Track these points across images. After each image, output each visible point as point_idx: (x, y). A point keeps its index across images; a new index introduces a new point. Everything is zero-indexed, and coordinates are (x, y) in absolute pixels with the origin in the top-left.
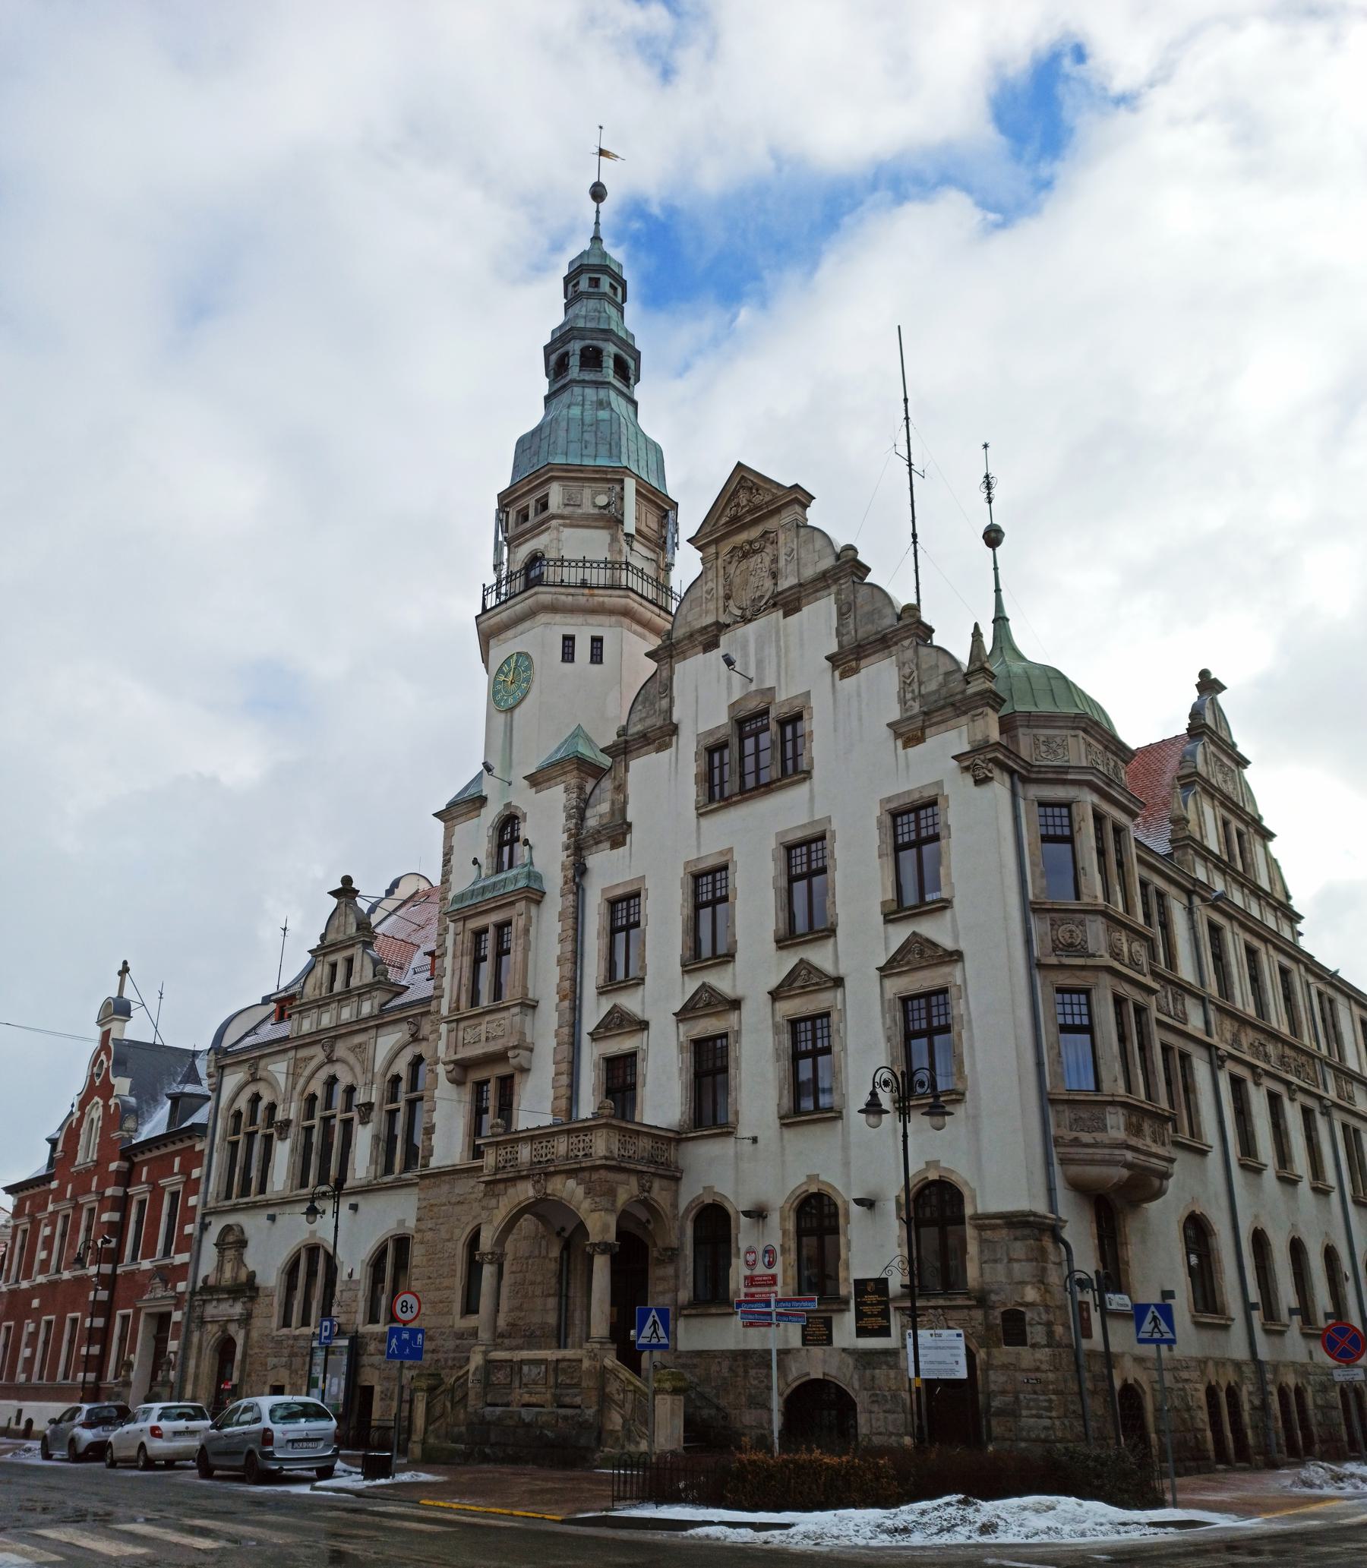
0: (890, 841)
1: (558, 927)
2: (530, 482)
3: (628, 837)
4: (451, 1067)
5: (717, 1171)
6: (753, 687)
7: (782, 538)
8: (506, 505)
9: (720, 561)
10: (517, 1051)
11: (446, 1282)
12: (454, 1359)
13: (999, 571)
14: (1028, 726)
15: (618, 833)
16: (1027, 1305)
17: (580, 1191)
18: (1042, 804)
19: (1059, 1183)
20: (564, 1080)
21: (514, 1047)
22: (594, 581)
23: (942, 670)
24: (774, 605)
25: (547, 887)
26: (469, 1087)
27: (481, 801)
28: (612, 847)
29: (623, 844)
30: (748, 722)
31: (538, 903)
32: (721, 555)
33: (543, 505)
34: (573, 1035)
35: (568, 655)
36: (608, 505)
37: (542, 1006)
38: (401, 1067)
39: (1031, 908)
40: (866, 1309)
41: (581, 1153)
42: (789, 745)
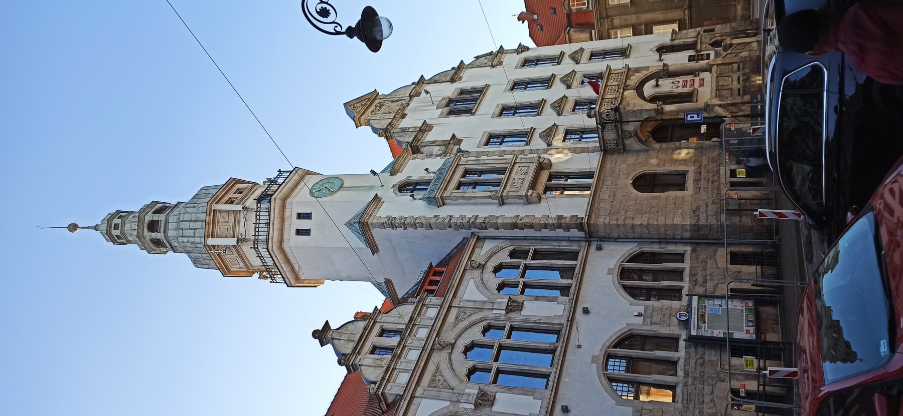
22: (267, 217)
35: (307, 232)
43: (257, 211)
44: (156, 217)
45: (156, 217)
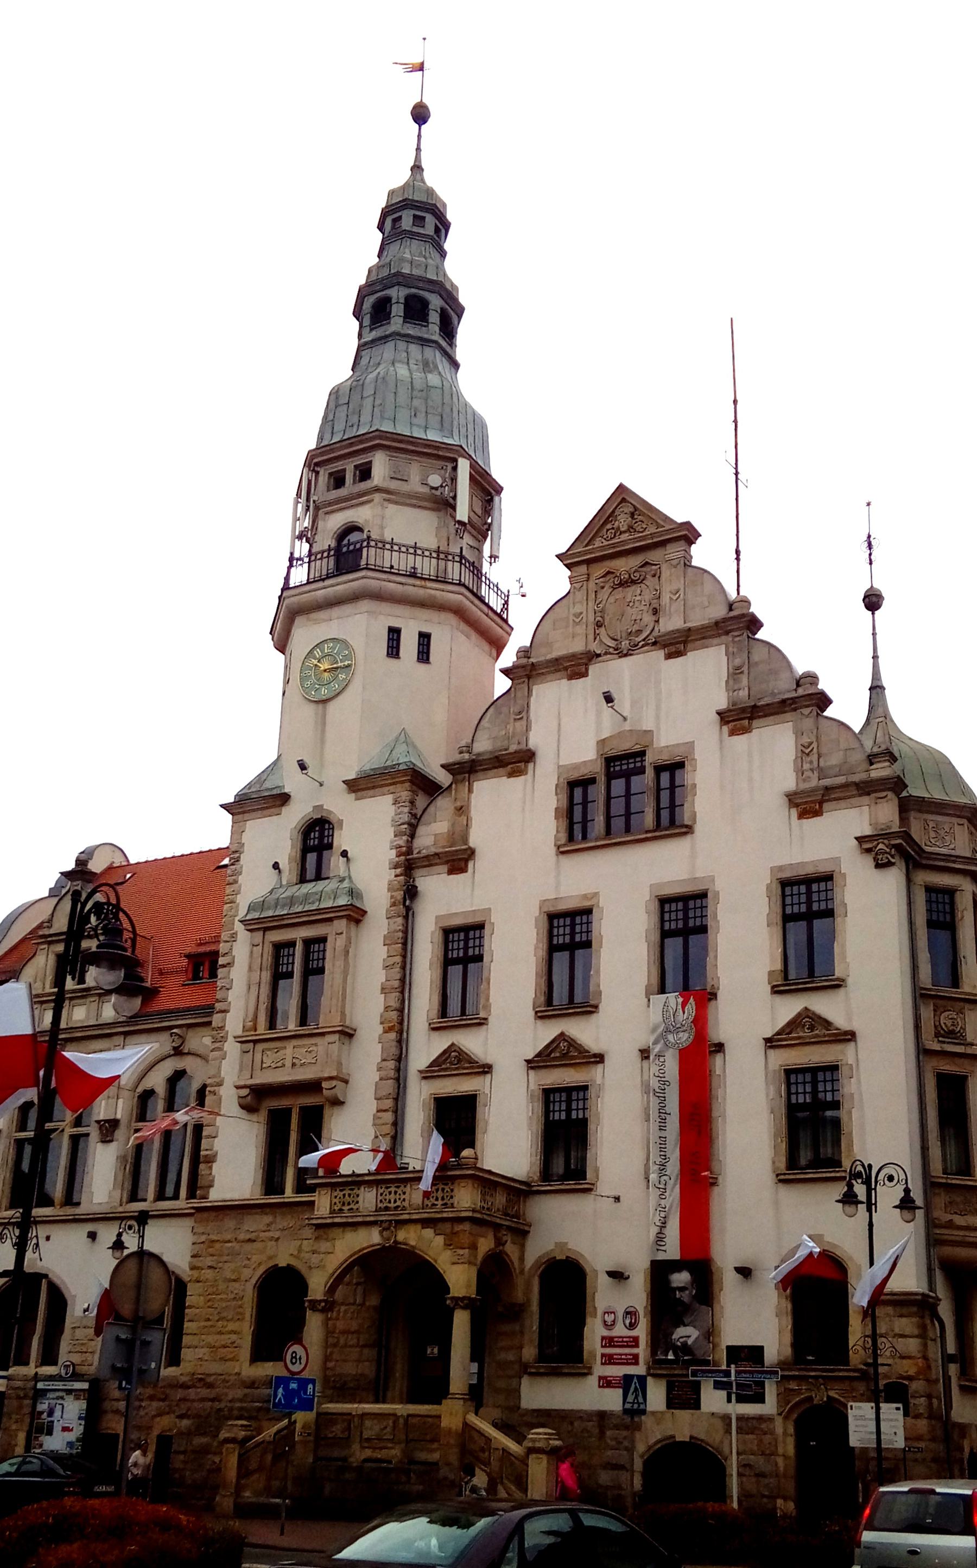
0: (778, 909)
1: (383, 952)
2: (351, 445)
3: (470, 864)
4: (245, 1092)
5: (561, 1225)
6: (627, 726)
7: (666, 572)
8: (317, 464)
9: (592, 584)
10: (334, 1083)
11: (231, 1326)
12: (241, 1409)
13: (878, 637)
14: (920, 811)
15: (458, 860)
16: (910, 1378)
17: (440, 1240)
18: (929, 889)
19: (936, 1264)
20: (389, 1117)
21: (331, 1078)
23: (843, 745)
24: (654, 644)
25: (367, 905)
26: (262, 1116)
27: (283, 799)
28: (451, 872)
29: (463, 870)
30: (622, 763)
31: (358, 922)
32: (593, 578)
33: (365, 473)
34: (398, 1070)
35: (394, 650)
36: (441, 486)
38: (157, 1081)
39: (920, 996)
41: (440, 1202)
42: (665, 795)
43: (438, 551)
44: (434, 317)
45: (434, 317)
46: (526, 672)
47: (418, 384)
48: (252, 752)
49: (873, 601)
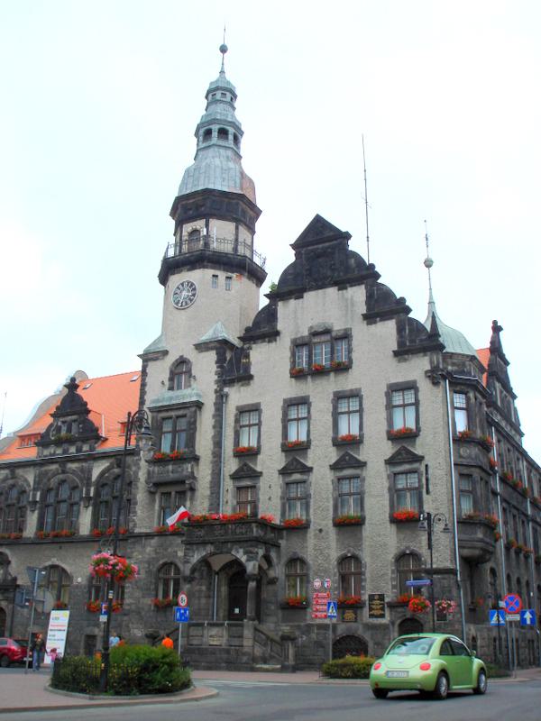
15: (246, 378)
27: (165, 353)
37: (202, 462)
40: (374, 607)
44: (231, 137)
45: (231, 137)
46: (275, 296)
47: (225, 167)
48: (149, 331)
49: (428, 264)
